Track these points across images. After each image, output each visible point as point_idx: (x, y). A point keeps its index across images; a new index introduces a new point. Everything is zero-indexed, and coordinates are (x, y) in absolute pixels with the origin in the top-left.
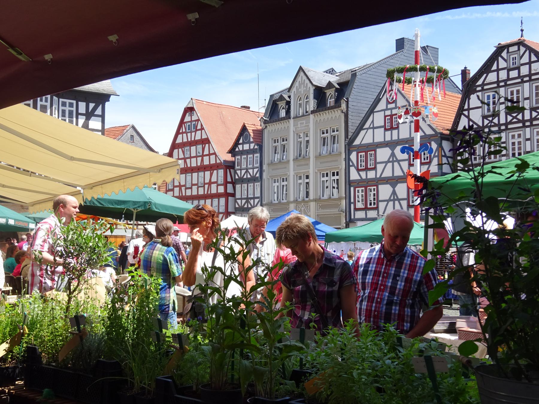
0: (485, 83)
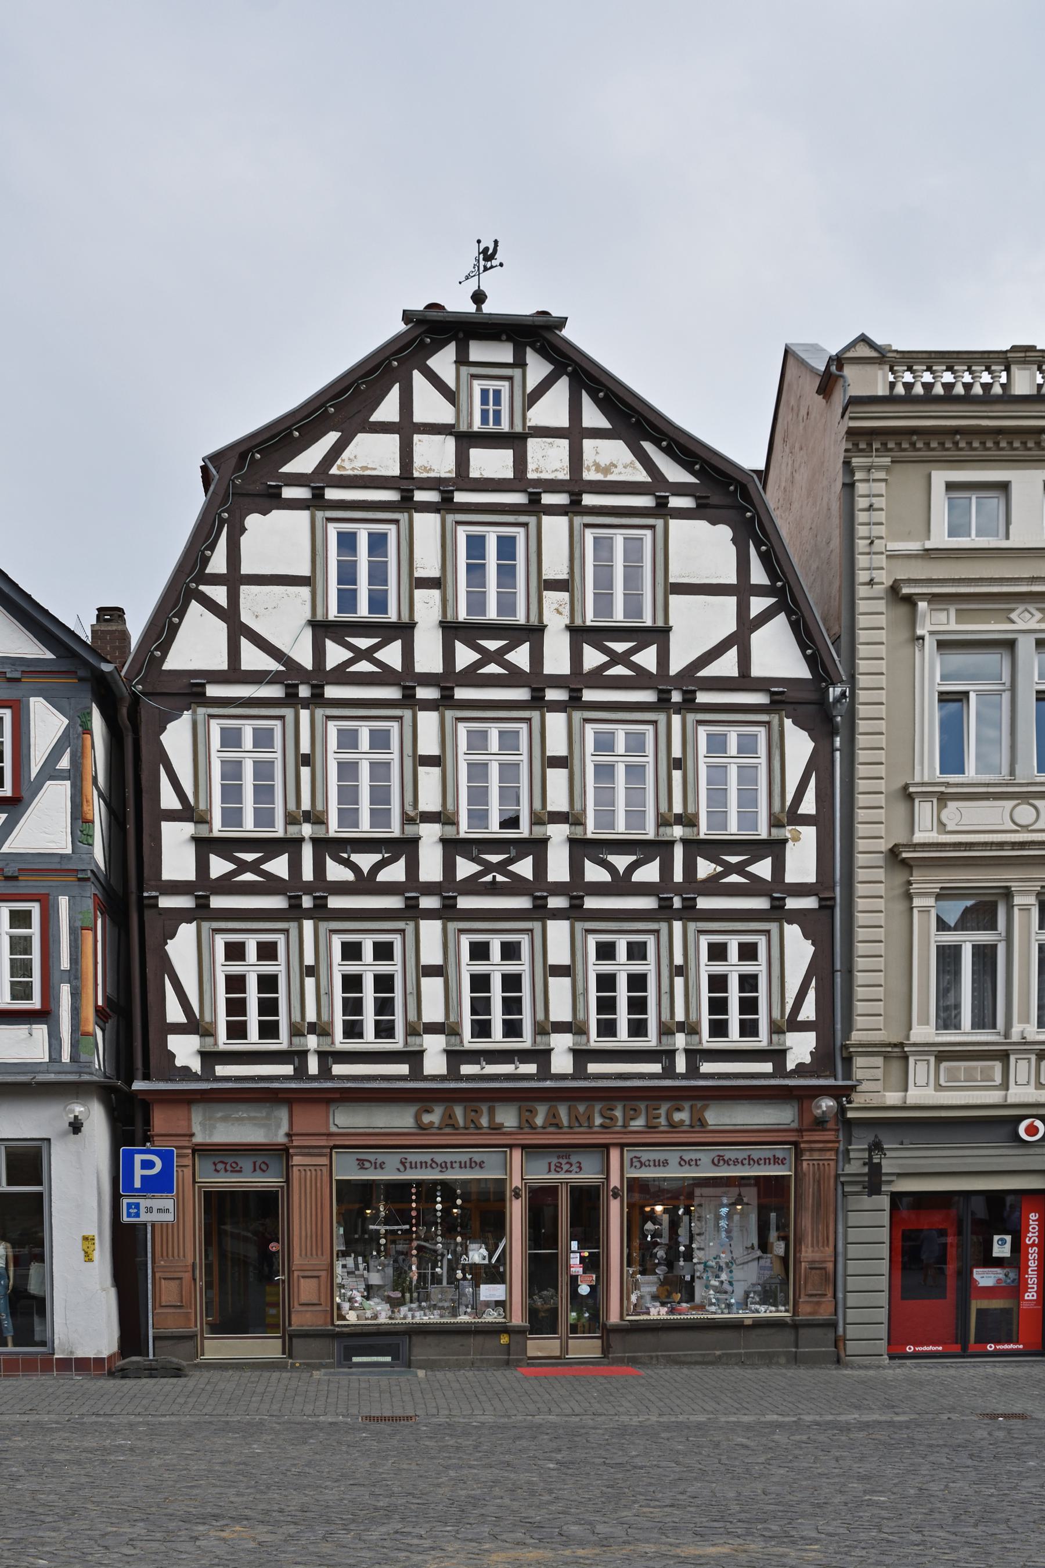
0: (334, 471)
